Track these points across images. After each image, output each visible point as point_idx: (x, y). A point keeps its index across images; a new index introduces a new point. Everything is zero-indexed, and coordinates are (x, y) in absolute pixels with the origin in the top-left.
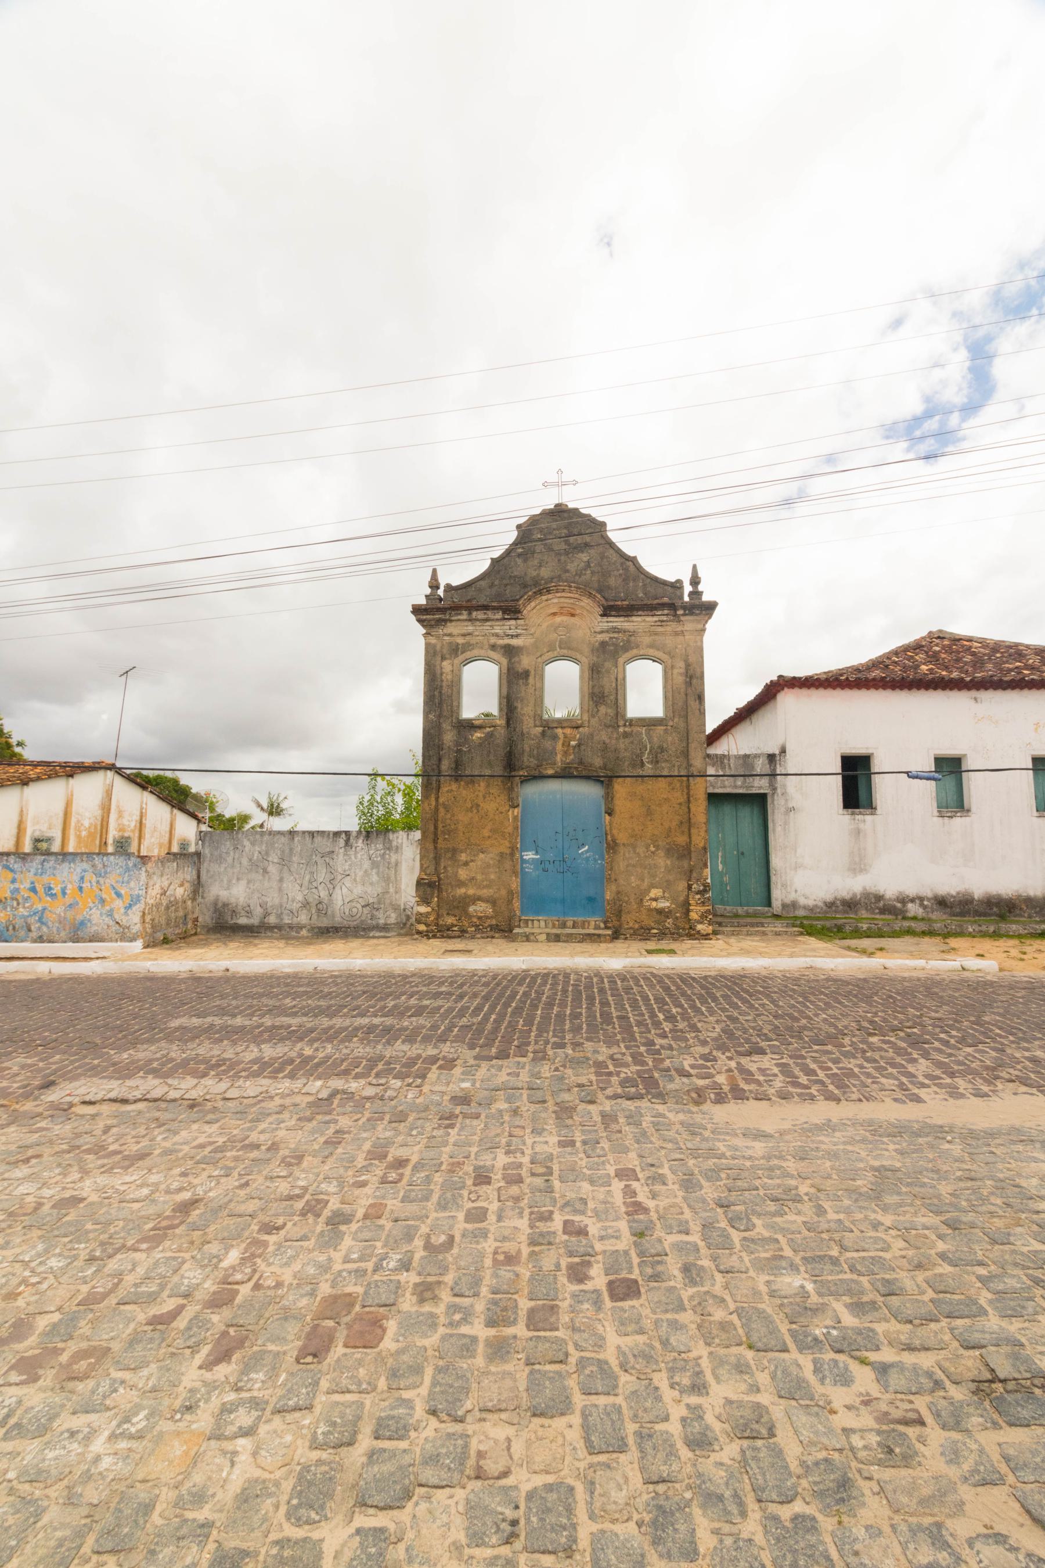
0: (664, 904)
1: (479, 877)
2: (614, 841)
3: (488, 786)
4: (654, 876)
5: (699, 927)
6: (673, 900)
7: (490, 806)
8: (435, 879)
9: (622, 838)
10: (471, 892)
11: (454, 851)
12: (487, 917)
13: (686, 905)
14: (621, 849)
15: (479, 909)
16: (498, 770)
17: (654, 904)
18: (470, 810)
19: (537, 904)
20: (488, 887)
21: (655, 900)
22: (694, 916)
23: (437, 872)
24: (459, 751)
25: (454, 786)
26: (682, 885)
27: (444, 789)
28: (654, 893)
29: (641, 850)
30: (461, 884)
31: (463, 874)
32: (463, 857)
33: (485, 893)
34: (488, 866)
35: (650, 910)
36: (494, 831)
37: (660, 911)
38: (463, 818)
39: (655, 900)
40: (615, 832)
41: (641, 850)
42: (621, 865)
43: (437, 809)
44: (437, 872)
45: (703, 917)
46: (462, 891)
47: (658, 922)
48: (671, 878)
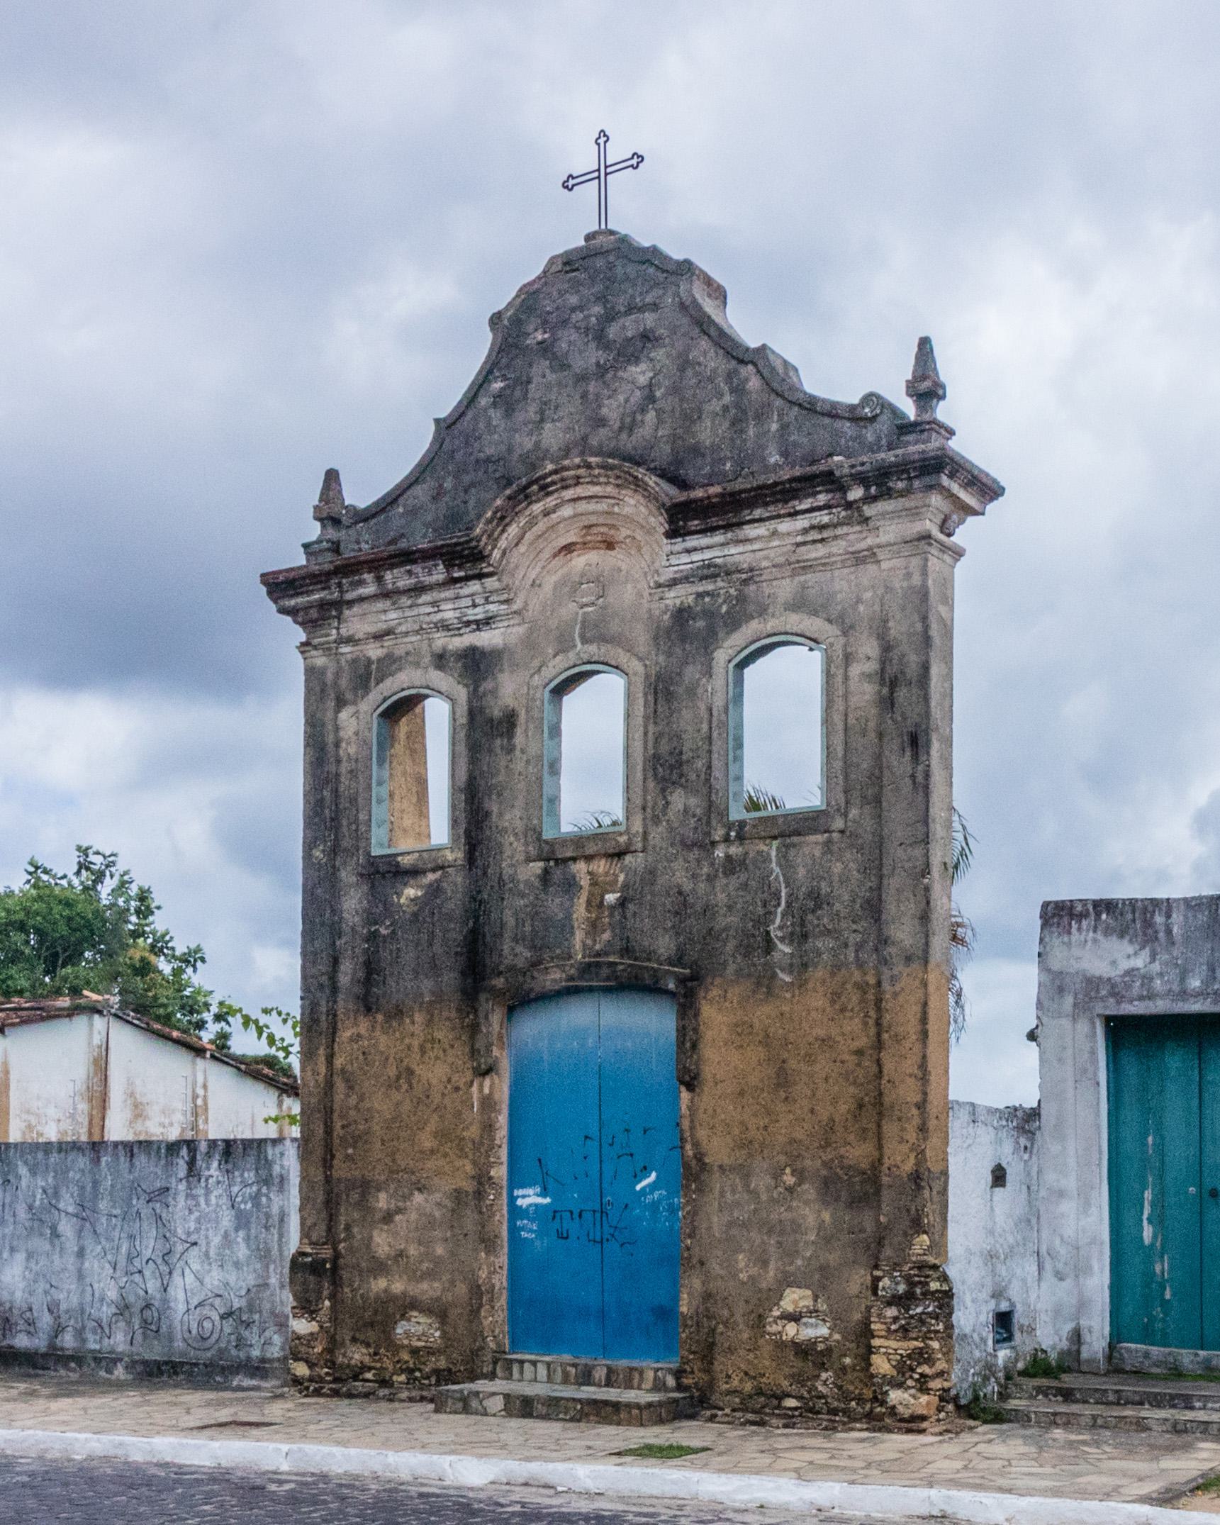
0: (815, 1331)
1: (413, 1251)
2: (699, 1157)
3: (429, 1023)
4: (789, 1254)
5: (895, 1396)
6: (837, 1320)
7: (434, 1073)
8: (327, 1253)
9: (718, 1150)
10: (398, 1287)
11: (366, 1187)
12: (430, 1351)
13: (865, 1333)
14: (716, 1182)
15: (416, 1329)
16: (450, 978)
17: (791, 1330)
18: (393, 1084)
19: (538, 1321)
20: (430, 1275)
21: (795, 1318)
22: (882, 1365)
23: (331, 1238)
24: (373, 937)
25: (363, 1026)
26: (857, 1279)
27: (345, 1034)
28: (794, 1298)
29: (761, 1182)
30: (379, 1268)
31: (382, 1242)
32: (382, 1201)
33: (427, 1290)
34: (431, 1223)
35: (781, 1345)
36: (443, 1135)
37: (804, 1350)
38: (381, 1104)
39: (795, 1318)
40: (702, 1134)
41: (761, 1182)
42: (715, 1221)
43: (330, 1085)
44: (331, 1238)
45: (904, 1368)
46: (379, 1285)
47: (799, 1379)
48: (833, 1258)
